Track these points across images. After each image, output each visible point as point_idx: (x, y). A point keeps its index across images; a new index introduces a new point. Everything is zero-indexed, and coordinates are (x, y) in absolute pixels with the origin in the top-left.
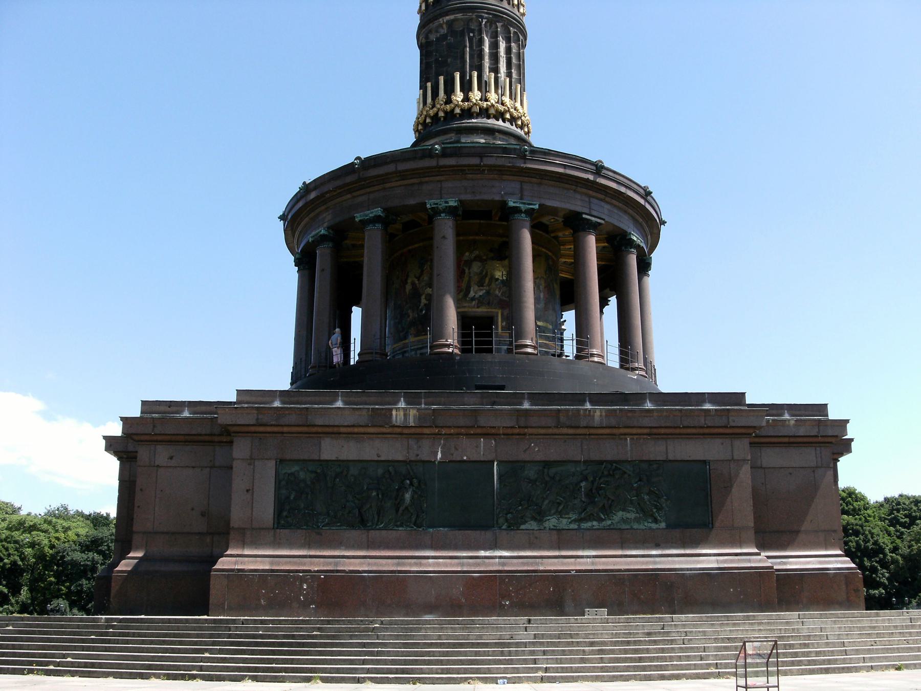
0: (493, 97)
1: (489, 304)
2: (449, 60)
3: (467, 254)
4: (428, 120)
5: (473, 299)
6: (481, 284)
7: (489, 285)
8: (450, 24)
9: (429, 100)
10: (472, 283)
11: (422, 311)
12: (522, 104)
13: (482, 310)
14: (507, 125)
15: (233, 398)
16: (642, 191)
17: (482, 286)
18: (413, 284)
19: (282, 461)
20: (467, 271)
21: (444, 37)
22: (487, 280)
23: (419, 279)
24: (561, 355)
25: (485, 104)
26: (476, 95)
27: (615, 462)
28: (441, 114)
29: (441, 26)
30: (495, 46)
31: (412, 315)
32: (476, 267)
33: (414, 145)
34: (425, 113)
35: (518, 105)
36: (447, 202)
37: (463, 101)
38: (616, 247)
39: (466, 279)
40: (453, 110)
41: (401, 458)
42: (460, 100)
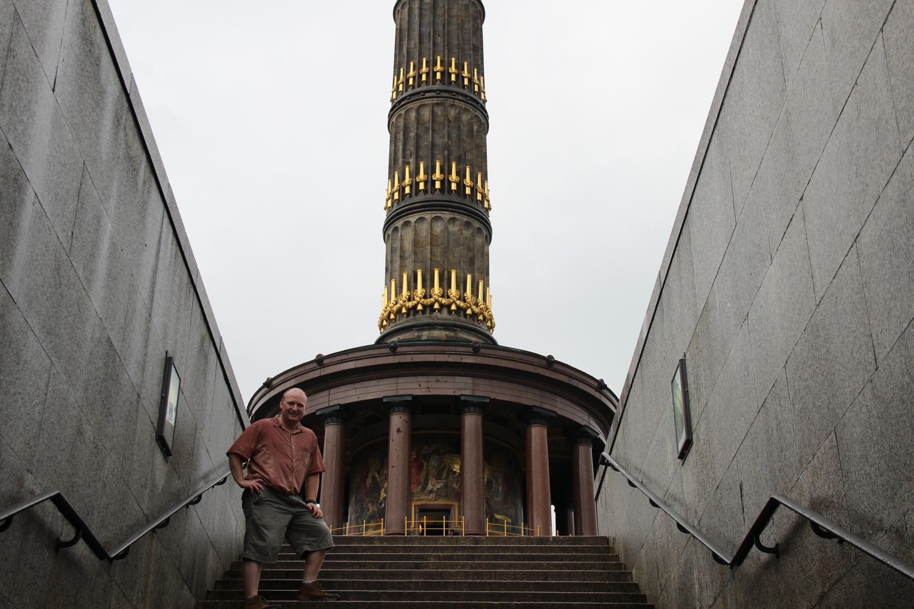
1: (446, 497)
3: (426, 447)
4: (392, 316)
5: (431, 492)
6: (438, 477)
7: (447, 478)
10: (430, 476)
11: (381, 504)
13: (441, 502)
16: (596, 384)
17: (440, 479)
18: (374, 478)
20: (425, 464)
22: (445, 474)
23: (379, 472)
25: (444, 301)
31: (372, 508)
32: (434, 462)
33: (380, 341)
34: (389, 309)
38: (567, 438)
39: (424, 473)
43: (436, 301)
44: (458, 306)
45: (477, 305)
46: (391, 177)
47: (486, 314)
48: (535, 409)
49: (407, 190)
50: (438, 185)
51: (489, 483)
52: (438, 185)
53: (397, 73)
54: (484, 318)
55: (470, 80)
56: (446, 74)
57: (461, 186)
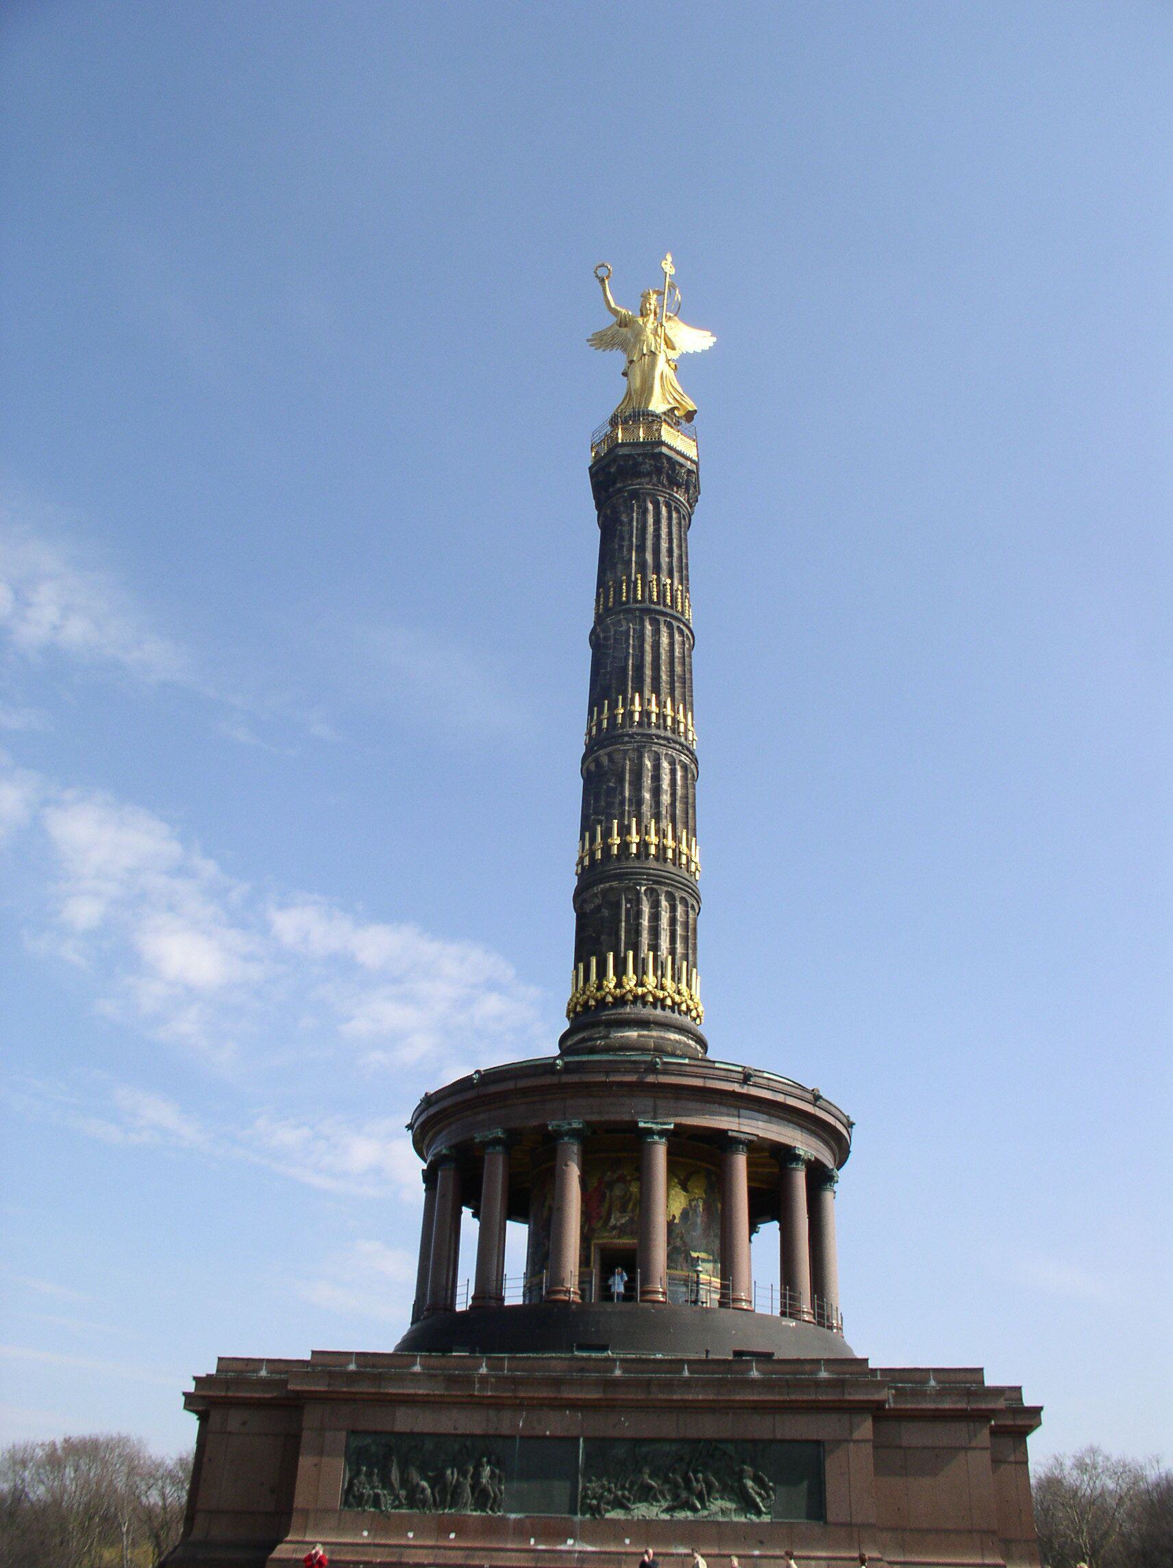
0: (651, 980)
1: (632, 1233)
2: (603, 937)
3: (609, 1173)
5: (614, 1228)
6: (623, 1210)
7: (633, 1211)
8: (605, 893)
9: (581, 984)
12: (689, 985)
13: (627, 1241)
14: (668, 1012)
15: (308, 1357)
19: (354, 1432)
20: (608, 1194)
21: (598, 909)
24: (695, 1302)
25: (640, 991)
26: (630, 980)
27: (716, 1440)
28: (592, 1002)
29: (595, 895)
30: (655, 917)
32: (618, 1191)
35: (683, 986)
36: (570, 1124)
37: (615, 987)
39: (606, 1205)
40: (604, 998)
41: (478, 1431)
42: (612, 985)
43: (630, 991)
44: (654, 996)
45: (679, 993)
46: (582, 838)
47: (690, 1002)
48: (730, 1133)
49: (599, 855)
50: (634, 849)
51: (685, 1214)
52: (634, 849)
53: (591, 713)
54: (688, 1007)
55: (674, 719)
56: (645, 714)
57: (662, 849)
